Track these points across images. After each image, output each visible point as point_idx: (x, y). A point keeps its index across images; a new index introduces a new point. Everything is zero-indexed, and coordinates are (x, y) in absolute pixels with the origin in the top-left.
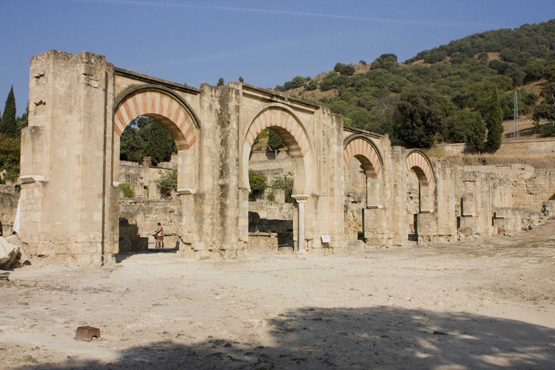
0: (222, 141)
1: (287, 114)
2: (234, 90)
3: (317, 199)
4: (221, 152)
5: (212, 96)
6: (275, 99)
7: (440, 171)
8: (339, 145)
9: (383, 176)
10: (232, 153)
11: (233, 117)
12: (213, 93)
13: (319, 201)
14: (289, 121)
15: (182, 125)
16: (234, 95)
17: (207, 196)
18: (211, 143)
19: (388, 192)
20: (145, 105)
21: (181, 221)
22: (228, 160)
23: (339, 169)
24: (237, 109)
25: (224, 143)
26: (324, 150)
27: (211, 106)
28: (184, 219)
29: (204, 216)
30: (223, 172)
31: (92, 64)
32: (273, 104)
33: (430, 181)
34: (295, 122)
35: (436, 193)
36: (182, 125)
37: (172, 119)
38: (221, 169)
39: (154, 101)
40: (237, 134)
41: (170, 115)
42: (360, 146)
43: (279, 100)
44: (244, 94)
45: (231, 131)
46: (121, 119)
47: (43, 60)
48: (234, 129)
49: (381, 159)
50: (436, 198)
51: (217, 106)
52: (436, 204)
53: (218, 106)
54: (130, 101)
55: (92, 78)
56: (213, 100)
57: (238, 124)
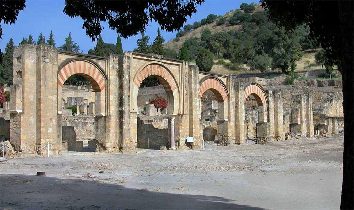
0: (120, 86)
1: (162, 67)
2: (127, 57)
3: (182, 117)
4: (120, 92)
5: (114, 61)
6: (153, 59)
7: (271, 96)
8: (195, 83)
9: (229, 100)
10: (126, 92)
11: (126, 72)
12: (115, 59)
13: (183, 118)
14: (163, 71)
15: (97, 78)
16: (126, 60)
17: (112, 117)
18: (114, 87)
19: (232, 111)
20: (75, 68)
21: (98, 132)
22: (123, 97)
23: (195, 99)
24: (129, 67)
25: (121, 87)
26: (186, 87)
27: (113, 66)
28: (99, 130)
29: (110, 129)
30: (121, 104)
31: (45, 50)
32: (152, 62)
33: (264, 103)
34: (167, 72)
35: (268, 110)
36: (97, 78)
37: (91, 75)
38: (119, 102)
39: (80, 66)
40: (129, 82)
41: (89, 73)
42: (211, 83)
43: (156, 60)
44: (134, 58)
45: (125, 80)
46: (62, 77)
47: (20, 49)
48: (127, 79)
49: (226, 90)
50: (268, 113)
51: (117, 66)
52: (268, 117)
53: (118, 66)
54: (67, 66)
55: (46, 58)
56: (114, 63)
57: (129, 76)
